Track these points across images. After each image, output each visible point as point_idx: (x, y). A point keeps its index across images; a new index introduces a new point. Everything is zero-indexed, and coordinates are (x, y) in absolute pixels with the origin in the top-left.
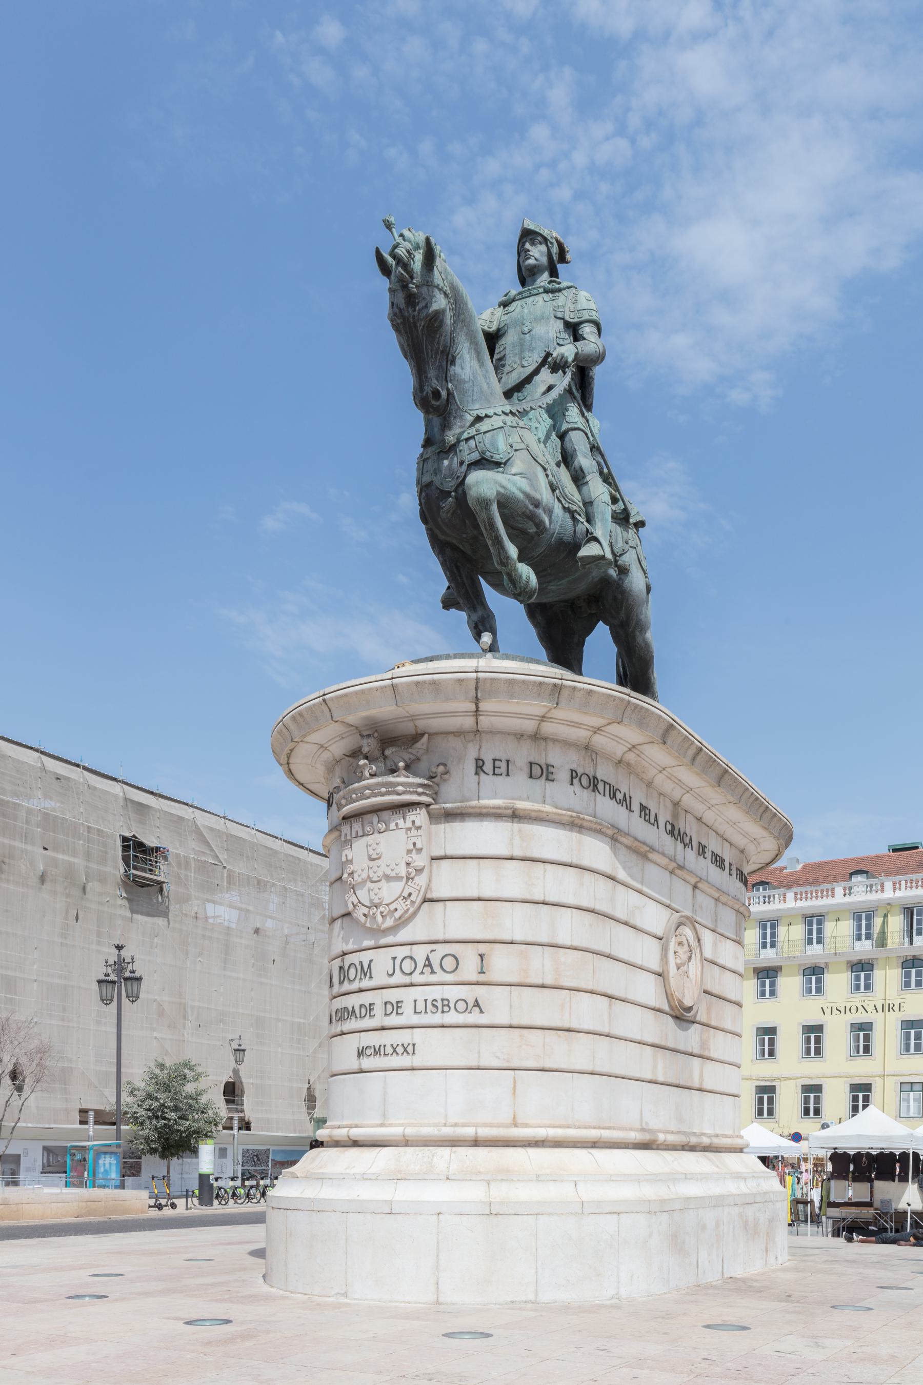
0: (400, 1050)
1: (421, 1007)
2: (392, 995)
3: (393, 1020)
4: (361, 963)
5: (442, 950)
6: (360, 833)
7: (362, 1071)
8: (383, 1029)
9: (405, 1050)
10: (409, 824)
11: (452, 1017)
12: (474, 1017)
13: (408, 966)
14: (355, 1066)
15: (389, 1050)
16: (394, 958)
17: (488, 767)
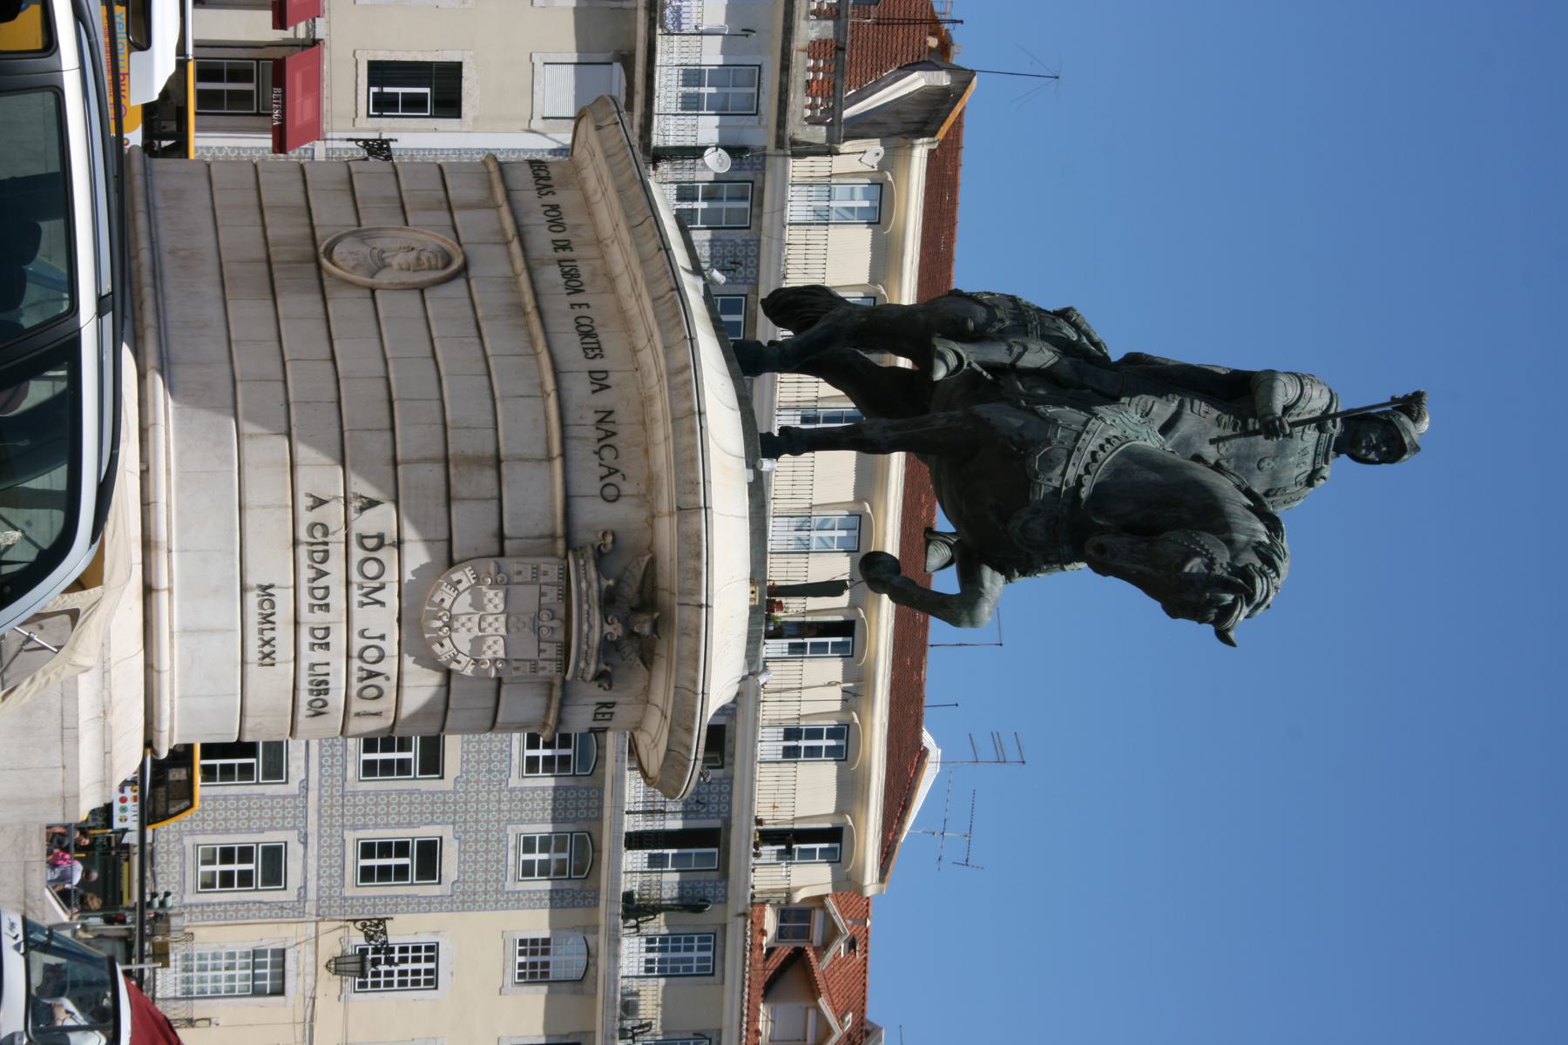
0: (267, 649)
1: (319, 670)
2: (338, 638)
3: (305, 639)
4: (382, 587)
5: (390, 688)
6: (544, 600)
7: (243, 590)
8: (296, 623)
9: (268, 655)
10: (541, 664)
11: (305, 697)
12: (303, 709)
13: (372, 654)
14: (252, 581)
15: (268, 635)
16: (382, 637)
17: (604, 710)
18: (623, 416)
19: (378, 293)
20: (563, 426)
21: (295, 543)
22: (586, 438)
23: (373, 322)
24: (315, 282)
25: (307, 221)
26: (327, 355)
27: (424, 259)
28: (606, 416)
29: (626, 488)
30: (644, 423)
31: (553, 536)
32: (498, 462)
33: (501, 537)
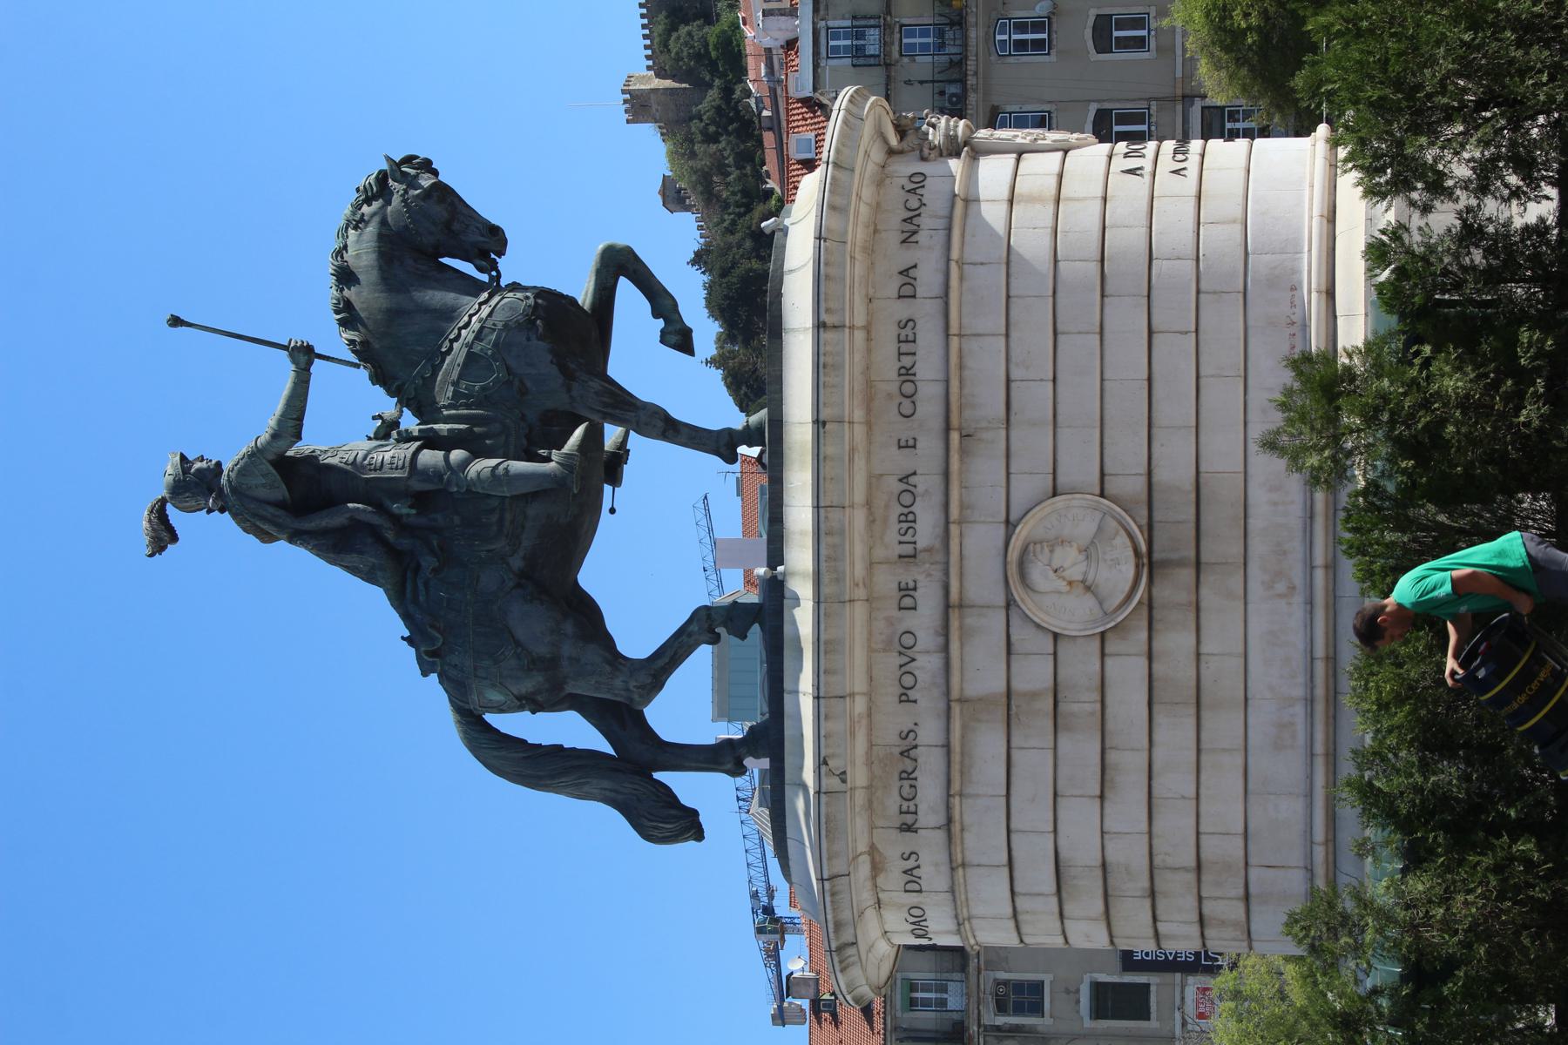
18: (892, 238)
19: (1097, 490)
20: (949, 229)
21: (1203, 156)
22: (931, 217)
23: (1107, 417)
24: (1156, 495)
25: (1155, 666)
26: (1157, 339)
27: (1046, 550)
28: (909, 238)
29: (905, 181)
30: (876, 231)
31: (960, 523)
32: (1011, 202)
33: (1018, 160)
